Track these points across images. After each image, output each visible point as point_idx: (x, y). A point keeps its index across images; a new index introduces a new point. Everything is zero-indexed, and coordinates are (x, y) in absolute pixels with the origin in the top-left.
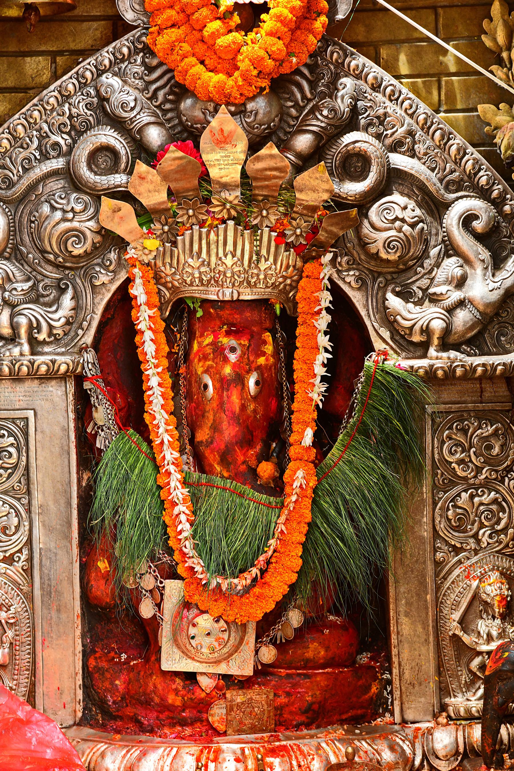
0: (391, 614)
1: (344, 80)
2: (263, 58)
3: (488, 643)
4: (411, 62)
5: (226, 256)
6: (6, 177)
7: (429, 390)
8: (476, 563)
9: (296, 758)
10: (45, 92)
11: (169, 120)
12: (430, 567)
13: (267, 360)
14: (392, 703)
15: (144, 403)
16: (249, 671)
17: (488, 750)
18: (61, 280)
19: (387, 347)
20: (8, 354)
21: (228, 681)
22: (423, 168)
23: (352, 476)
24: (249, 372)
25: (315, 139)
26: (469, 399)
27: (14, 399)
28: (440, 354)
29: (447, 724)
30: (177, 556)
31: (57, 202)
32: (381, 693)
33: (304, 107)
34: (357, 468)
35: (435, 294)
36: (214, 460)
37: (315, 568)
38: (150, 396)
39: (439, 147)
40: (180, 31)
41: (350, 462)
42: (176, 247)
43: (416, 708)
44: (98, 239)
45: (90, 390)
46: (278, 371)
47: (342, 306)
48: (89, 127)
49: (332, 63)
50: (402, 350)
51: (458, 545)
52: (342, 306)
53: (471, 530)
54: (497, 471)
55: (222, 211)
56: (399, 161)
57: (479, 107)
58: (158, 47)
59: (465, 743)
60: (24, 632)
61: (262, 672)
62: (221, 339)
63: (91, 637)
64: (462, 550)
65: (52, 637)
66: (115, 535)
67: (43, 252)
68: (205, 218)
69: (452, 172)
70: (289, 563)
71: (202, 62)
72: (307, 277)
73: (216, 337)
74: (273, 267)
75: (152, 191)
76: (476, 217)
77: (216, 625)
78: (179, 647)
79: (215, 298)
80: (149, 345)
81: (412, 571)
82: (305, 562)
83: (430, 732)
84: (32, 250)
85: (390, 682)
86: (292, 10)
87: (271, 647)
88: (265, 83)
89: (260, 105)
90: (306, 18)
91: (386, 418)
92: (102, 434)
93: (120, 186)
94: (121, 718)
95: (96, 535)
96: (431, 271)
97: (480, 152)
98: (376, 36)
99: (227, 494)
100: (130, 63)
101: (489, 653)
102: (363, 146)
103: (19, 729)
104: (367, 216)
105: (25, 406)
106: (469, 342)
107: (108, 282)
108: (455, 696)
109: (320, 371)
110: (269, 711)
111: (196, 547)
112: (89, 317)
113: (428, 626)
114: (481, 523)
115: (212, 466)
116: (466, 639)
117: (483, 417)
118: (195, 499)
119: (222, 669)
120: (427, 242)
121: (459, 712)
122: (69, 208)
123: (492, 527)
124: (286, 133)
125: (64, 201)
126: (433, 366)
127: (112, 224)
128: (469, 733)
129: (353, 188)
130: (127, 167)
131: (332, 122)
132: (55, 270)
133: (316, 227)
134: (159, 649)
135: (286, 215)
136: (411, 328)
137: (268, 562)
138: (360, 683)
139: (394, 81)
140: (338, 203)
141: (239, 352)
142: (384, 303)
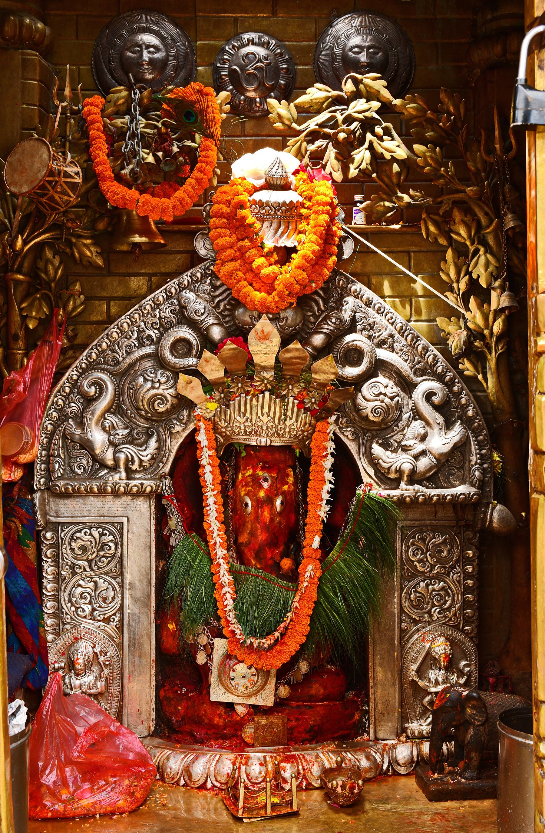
1: (346, 299)
2: (292, 284)
3: (436, 687)
4: (392, 287)
6: (115, 357)
8: (429, 631)
9: (302, 763)
10: (143, 301)
11: (227, 322)
13: (289, 487)
15: (204, 515)
16: (270, 703)
17: (434, 761)
18: (149, 428)
19: (372, 481)
20: (111, 478)
21: (256, 709)
24: (277, 495)
25: (326, 338)
26: (427, 518)
28: (408, 487)
29: (406, 742)
30: (223, 622)
31: (148, 376)
32: (361, 719)
33: (319, 316)
36: (251, 556)
37: (319, 632)
39: (410, 345)
40: (237, 264)
42: (229, 408)
44: (175, 401)
46: (296, 495)
47: (342, 453)
48: (172, 326)
49: (339, 287)
51: (417, 618)
52: (342, 453)
53: (426, 608)
54: (445, 568)
55: (261, 385)
56: (383, 354)
58: (222, 273)
59: (418, 755)
63: (162, 676)
64: (419, 621)
66: (181, 607)
67: (138, 409)
68: (249, 389)
69: (419, 363)
71: (251, 285)
73: (254, 471)
74: (295, 424)
75: (214, 369)
76: (434, 394)
79: (254, 444)
80: (209, 475)
83: (394, 746)
85: (367, 712)
87: (287, 686)
88: (293, 300)
89: (289, 314)
90: (322, 257)
93: (192, 366)
95: (168, 606)
97: (437, 349)
100: (202, 283)
101: (436, 693)
102: (359, 344)
104: (360, 391)
106: (429, 479)
108: (412, 722)
109: (326, 496)
110: (284, 731)
111: (236, 617)
116: (421, 683)
117: (436, 530)
118: (237, 583)
119: (253, 701)
120: (401, 410)
122: (157, 380)
123: (441, 606)
124: (307, 333)
127: (185, 392)
128: (421, 748)
129: (351, 372)
130: (197, 353)
135: (305, 389)
137: (286, 628)
139: (381, 301)
140: (342, 381)
141: (270, 482)
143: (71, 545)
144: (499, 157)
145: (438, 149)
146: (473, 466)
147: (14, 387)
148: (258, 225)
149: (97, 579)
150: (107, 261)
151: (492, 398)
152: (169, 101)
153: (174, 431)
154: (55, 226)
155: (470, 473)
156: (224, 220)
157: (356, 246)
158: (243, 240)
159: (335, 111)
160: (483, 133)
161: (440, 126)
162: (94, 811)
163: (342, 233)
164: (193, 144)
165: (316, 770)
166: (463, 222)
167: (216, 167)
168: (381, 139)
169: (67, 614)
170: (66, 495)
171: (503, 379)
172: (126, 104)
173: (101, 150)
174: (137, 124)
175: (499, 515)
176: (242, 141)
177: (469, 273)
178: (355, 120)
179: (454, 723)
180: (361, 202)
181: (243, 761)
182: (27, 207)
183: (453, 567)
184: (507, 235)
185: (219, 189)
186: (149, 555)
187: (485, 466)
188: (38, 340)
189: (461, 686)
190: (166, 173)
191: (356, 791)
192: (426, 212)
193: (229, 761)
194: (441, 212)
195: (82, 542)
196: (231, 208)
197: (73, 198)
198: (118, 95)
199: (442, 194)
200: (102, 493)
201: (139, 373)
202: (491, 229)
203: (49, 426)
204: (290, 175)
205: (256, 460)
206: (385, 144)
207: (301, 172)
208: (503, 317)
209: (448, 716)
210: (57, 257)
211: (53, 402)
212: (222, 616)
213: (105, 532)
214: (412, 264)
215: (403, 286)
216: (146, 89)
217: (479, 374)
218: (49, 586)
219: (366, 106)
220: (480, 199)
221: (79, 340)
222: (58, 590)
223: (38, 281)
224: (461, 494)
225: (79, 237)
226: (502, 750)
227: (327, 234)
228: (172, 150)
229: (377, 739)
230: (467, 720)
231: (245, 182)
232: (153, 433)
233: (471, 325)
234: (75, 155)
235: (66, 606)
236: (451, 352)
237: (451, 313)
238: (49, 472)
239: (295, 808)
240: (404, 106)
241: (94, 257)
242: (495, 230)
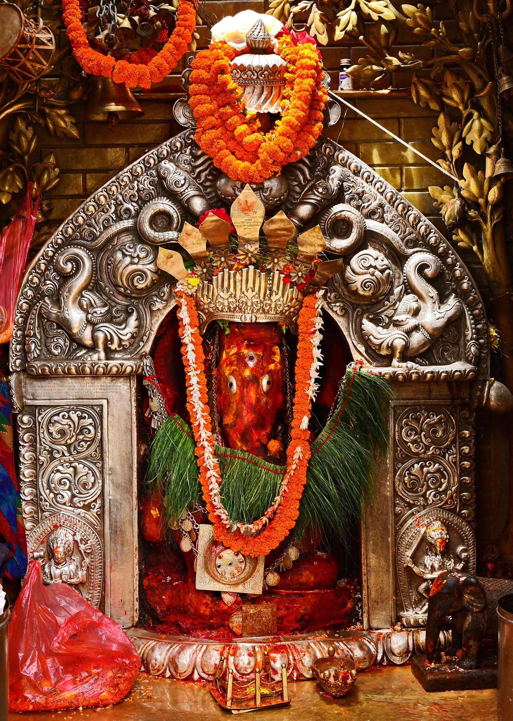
1: (333, 167)
2: (276, 151)
4: (381, 156)
6: (92, 233)
7: (393, 390)
8: (424, 515)
9: (292, 654)
10: (121, 173)
11: (208, 194)
12: (391, 518)
13: (276, 366)
15: (187, 396)
16: (259, 591)
17: (430, 650)
18: (128, 306)
19: (363, 358)
20: (89, 359)
23: (336, 451)
24: (262, 374)
25: (313, 209)
26: (421, 396)
27: (93, 391)
28: (401, 364)
29: (401, 631)
30: (208, 507)
32: (354, 608)
33: (305, 186)
34: (340, 446)
35: (397, 320)
36: (237, 438)
37: (309, 517)
38: (191, 391)
39: (401, 215)
40: (218, 132)
41: (335, 441)
44: (155, 277)
45: (148, 386)
46: (283, 374)
47: (330, 328)
50: (373, 360)
51: (412, 502)
52: (330, 328)
53: (421, 491)
54: (440, 449)
55: (245, 258)
56: (373, 225)
57: (429, 188)
58: (202, 142)
59: (413, 644)
60: (97, 560)
61: (269, 592)
62: (242, 351)
63: (145, 565)
64: (414, 505)
65: (117, 564)
66: (164, 491)
67: (116, 286)
68: (233, 263)
69: (410, 234)
70: (289, 514)
71: (233, 154)
72: (306, 306)
73: (239, 349)
74: (282, 299)
75: (195, 242)
76: (427, 266)
77: (236, 558)
78: (208, 572)
79: (239, 320)
80: (191, 354)
81: (378, 520)
83: (389, 636)
84: (108, 284)
85: (360, 600)
86: (298, 118)
87: (276, 574)
88: (278, 169)
89: (273, 185)
90: (307, 124)
91: (362, 410)
92: (156, 418)
93: (172, 240)
94: (166, 623)
95: (151, 491)
96: (394, 304)
97: (430, 220)
98: (356, 136)
101: (432, 580)
102: (347, 214)
103: (93, 629)
104: (349, 264)
105: (102, 397)
106: (422, 356)
107: (162, 309)
108: (407, 611)
109: (314, 375)
110: (273, 620)
111: (222, 501)
112: (148, 333)
113: (389, 560)
114: (428, 486)
116: (416, 570)
117: (431, 409)
118: (222, 466)
119: (240, 589)
120: (392, 283)
121: (410, 622)
122: (136, 255)
123: (436, 489)
124: (292, 204)
125: (132, 250)
126: (395, 372)
128: (417, 637)
129: (340, 244)
130: (177, 226)
131: (325, 197)
132: (124, 299)
133: (313, 271)
135: (291, 262)
136: (380, 345)
137: (274, 513)
140: (329, 254)
141: (255, 360)
142: (361, 326)
143: (48, 429)
145: (428, 9)
146: (468, 341)
148: (239, 91)
150: (82, 132)
151: (488, 270)
153: (155, 309)
154: (27, 97)
155: (465, 349)
156: (204, 85)
157: (343, 113)
158: (224, 106)
162: (76, 703)
163: (329, 98)
164: (170, 8)
165: (307, 661)
166: (456, 85)
167: (195, 31)
170: (43, 377)
171: (499, 250)
175: (497, 393)
176: (222, 4)
177: (462, 139)
179: (451, 610)
180: (347, 67)
181: (231, 652)
183: (448, 448)
184: (502, 100)
185: (198, 54)
186: (130, 438)
187: (482, 341)
188: (12, 216)
189: (458, 571)
190: (143, 38)
191: (349, 681)
192: (416, 76)
193: (216, 652)
195: (60, 426)
199: (433, 56)
200: (80, 374)
201: (117, 248)
202: (485, 92)
203: (24, 304)
204: (273, 38)
205: (241, 338)
207: (284, 35)
208: (499, 185)
209: (445, 603)
211: (28, 280)
212: (207, 501)
213: (84, 414)
214: (402, 131)
215: (393, 154)
217: (474, 245)
218: (27, 472)
220: (472, 61)
221: (54, 216)
222: (36, 477)
223: (11, 154)
224: (456, 371)
225: (53, 107)
229: (370, 629)
230: (465, 607)
231: (225, 46)
233: (464, 193)
234: (47, 21)
235: (45, 493)
236: (444, 222)
237: (444, 182)
238: (25, 353)
239: (286, 699)
241: (69, 128)
242: (489, 94)
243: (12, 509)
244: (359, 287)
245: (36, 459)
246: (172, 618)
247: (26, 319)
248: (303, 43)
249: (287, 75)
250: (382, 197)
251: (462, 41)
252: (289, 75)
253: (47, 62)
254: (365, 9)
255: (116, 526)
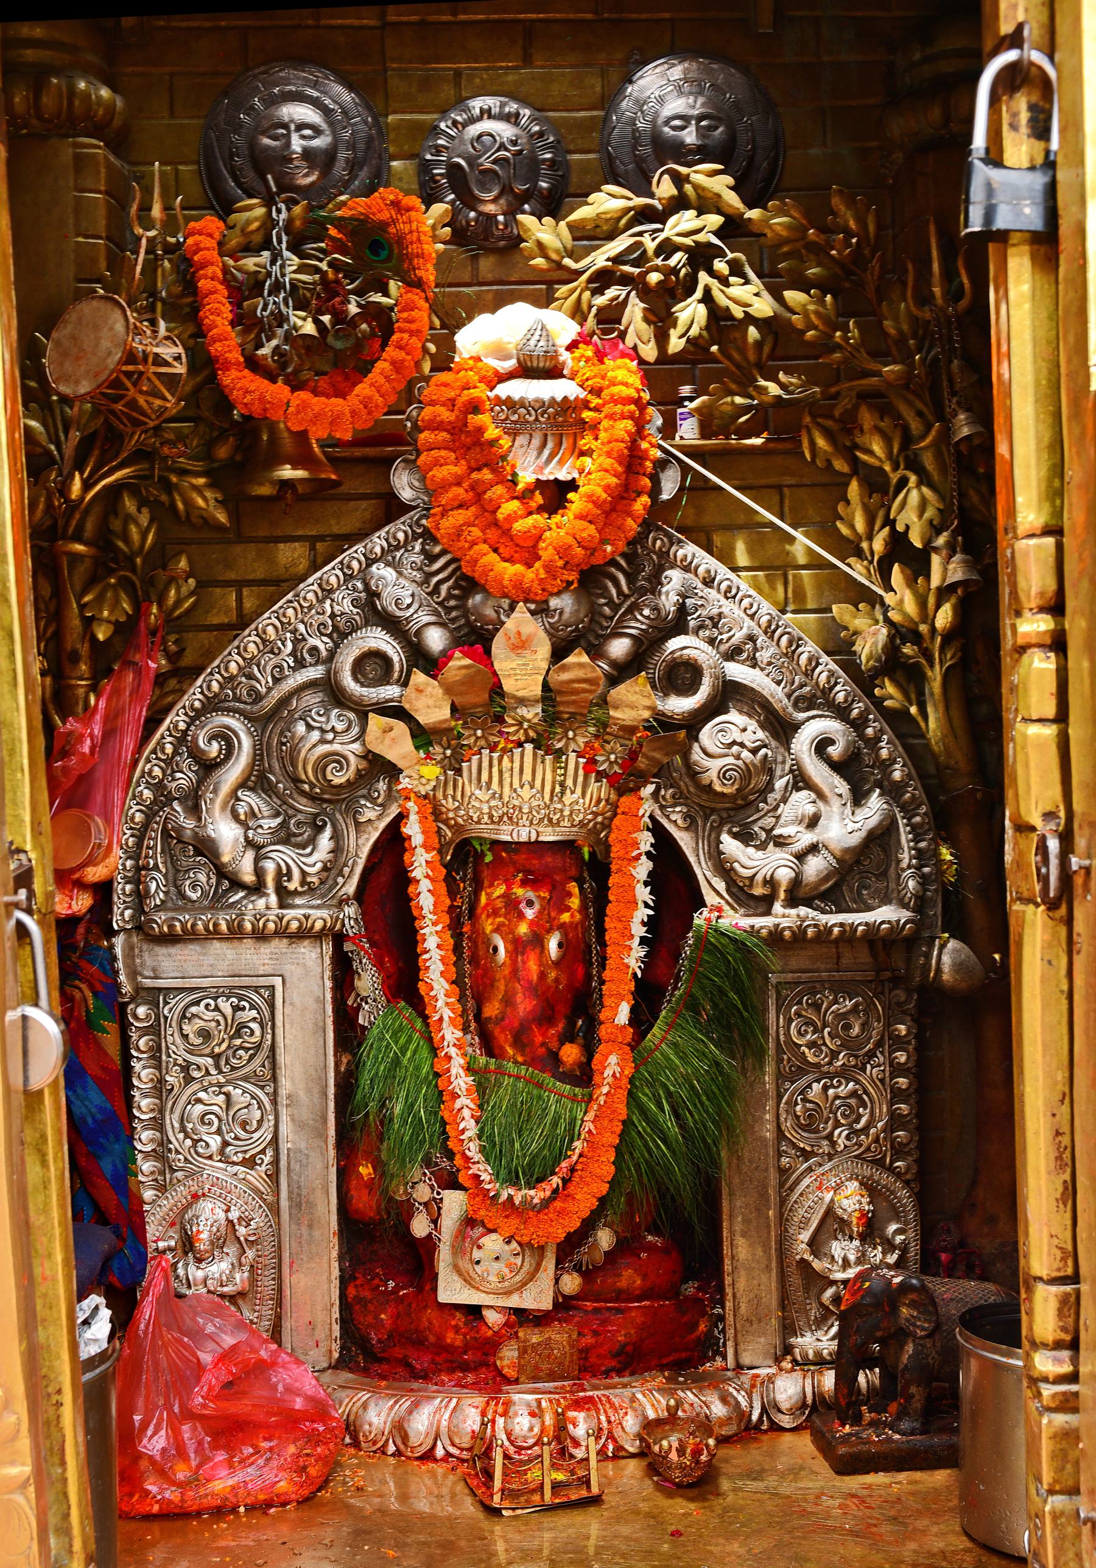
0: (725, 1234)
1: (668, 573)
4: (751, 552)
5: (522, 787)
6: (252, 689)
9: (605, 1411)
10: (302, 586)
11: (453, 620)
12: (773, 1177)
13: (572, 916)
14: (725, 1344)
15: (418, 969)
16: (546, 1304)
17: (843, 1402)
18: (316, 815)
20: (250, 906)
21: (521, 1317)
22: (767, 681)
23: (677, 1062)
24: (549, 931)
25: (634, 645)
26: (823, 966)
28: (788, 911)
29: (793, 1370)
30: (458, 1161)
32: (710, 1332)
33: (620, 606)
35: (781, 836)
37: (631, 1175)
39: (786, 655)
43: (755, 1351)
44: (363, 765)
46: (586, 930)
47: (666, 853)
51: (808, 1149)
52: (666, 853)
53: (824, 1129)
54: (856, 1057)
55: (517, 731)
56: (737, 671)
57: (834, 607)
61: (564, 1305)
63: (350, 1261)
64: (813, 1154)
66: (382, 1134)
67: (296, 781)
69: (801, 686)
71: (495, 550)
73: (509, 888)
75: (431, 704)
76: (832, 742)
77: (506, 1247)
79: (509, 838)
80: (426, 897)
82: (618, 1169)
83: (771, 1379)
85: (722, 1318)
86: (607, 488)
87: (575, 1275)
88: (573, 576)
89: (564, 603)
90: (623, 498)
92: (367, 1007)
93: (392, 700)
94: (387, 1360)
97: (835, 661)
98: (708, 519)
99: (521, 1085)
101: (845, 1282)
104: (697, 740)
106: (824, 896)
107: (375, 820)
108: (802, 1336)
109: (639, 930)
110: (572, 1355)
111: (482, 1150)
115: (502, 1048)
116: (817, 1265)
117: (842, 988)
118: (482, 1090)
119: (514, 1301)
120: (771, 772)
123: (850, 1126)
124: (598, 636)
125: (323, 719)
128: (819, 1381)
129: (680, 705)
131: (654, 623)
132: (310, 803)
134: (435, 1277)
135: (596, 737)
137: (572, 1170)
138: (685, 1319)
140: (663, 723)
141: (537, 906)
143: (181, 1029)
144: (941, 309)
145: (829, 298)
146: (903, 870)
147: (74, 746)
148: (505, 442)
149: (230, 1088)
150: (235, 515)
151: (936, 748)
152: (339, 223)
154: (140, 455)
155: (899, 885)
156: (444, 434)
157: (684, 479)
158: (479, 469)
159: (640, 234)
160: (910, 267)
161: (832, 256)
162: (234, 1500)
165: (631, 1424)
166: (877, 429)
168: (724, 282)
169: (178, 1152)
170: (170, 939)
171: (955, 713)
172: (262, 231)
173: (218, 313)
174: (282, 266)
175: (953, 959)
177: (890, 523)
178: (677, 248)
179: (879, 1334)
181: (500, 1409)
182: (88, 421)
183: (871, 1055)
185: (433, 380)
187: (926, 870)
188: (114, 661)
189: (889, 1267)
191: (703, 1458)
192: (810, 414)
194: (837, 413)
195: (202, 1023)
196: (456, 412)
197: (171, 403)
198: (248, 214)
199: (837, 380)
200: (236, 933)
203: (138, 814)
204: (562, 350)
206: (733, 291)
207: (581, 345)
208: (953, 600)
209: (867, 1323)
210: (145, 510)
211: (143, 772)
212: (455, 1150)
214: (786, 510)
215: (771, 549)
216: (297, 203)
218: (145, 1103)
219: (696, 224)
220: (906, 387)
221: (188, 660)
222: (161, 1111)
224: (883, 922)
225: (183, 472)
226: (967, 1379)
227: (631, 456)
228: (346, 311)
229: (739, 1367)
230: (901, 1329)
231: (480, 364)
232: (325, 824)
234: (173, 325)
235: (176, 1139)
237: (859, 595)
238: (140, 897)
239: (595, 1490)
240: (765, 221)
241: (211, 509)
242: (935, 444)
243: (120, 1166)
244: (715, 780)
245: (161, 1081)
246: (398, 1352)
247: (140, 839)
248: (614, 359)
249: (587, 415)
250: (753, 624)
251: (888, 353)
252: (590, 413)
253: (173, 395)
254: (721, 300)
255: (299, 1195)
